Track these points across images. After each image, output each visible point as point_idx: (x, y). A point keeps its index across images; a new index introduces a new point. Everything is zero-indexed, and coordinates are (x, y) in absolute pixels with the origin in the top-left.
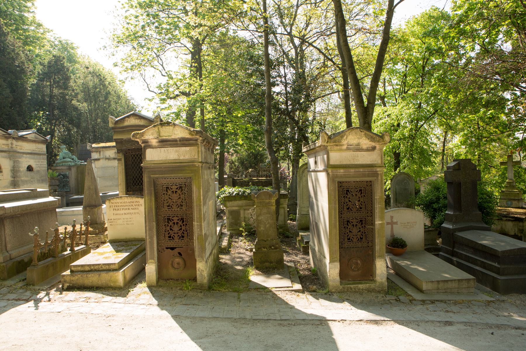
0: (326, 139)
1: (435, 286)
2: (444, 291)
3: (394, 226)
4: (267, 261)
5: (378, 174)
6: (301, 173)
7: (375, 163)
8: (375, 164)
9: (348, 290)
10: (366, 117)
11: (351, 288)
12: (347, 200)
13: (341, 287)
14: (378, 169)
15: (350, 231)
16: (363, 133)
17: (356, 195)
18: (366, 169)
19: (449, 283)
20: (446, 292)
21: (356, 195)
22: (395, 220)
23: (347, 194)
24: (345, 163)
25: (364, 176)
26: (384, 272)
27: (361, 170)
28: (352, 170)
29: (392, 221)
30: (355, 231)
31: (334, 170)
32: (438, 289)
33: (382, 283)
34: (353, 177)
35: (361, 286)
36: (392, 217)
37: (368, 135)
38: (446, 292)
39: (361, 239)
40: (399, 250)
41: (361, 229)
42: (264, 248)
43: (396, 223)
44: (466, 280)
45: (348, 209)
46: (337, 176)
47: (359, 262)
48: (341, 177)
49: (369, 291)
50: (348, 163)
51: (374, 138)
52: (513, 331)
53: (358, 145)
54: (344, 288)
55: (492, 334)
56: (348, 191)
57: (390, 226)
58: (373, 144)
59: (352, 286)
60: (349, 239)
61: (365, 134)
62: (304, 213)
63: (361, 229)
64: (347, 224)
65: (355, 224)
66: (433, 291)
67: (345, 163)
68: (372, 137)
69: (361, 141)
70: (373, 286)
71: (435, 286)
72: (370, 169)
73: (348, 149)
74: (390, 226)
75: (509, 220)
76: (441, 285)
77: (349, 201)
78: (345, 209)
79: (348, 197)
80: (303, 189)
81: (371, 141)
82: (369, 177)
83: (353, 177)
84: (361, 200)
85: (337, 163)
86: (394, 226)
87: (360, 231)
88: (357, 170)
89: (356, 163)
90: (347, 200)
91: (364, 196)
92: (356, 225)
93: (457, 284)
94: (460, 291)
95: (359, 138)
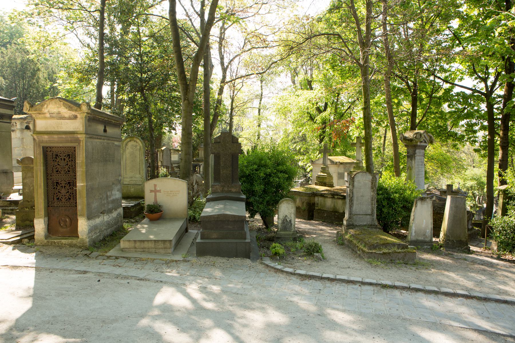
0: (28, 108)
1: (132, 245)
2: (142, 250)
3: (158, 194)
4: (27, 220)
5: (80, 140)
6: (124, 146)
7: (78, 130)
8: (77, 131)
9: (51, 244)
10: (186, 94)
11: (55, 243)
12: (56, 164)
13: (46, 241)
14: (79, 136)
15: (59, 192)
16: (62, 103)
17: (64, 159)
18: (69, 136)
19: (146, 243)
20: (143, 251)
21: (64, 159)
22: (158, 189)
23: (56, 158)
24: (50, 130)
25: (67, 142)
26: (84, 229)
27: (64, 136)
28: (56, 136)
29: (155, 189)
30: (63, 191)
31: (40, 136)
32: (135, 248)
33: (82, 240)
34: (57, 142)
35: (64, 241)
36: (155, 186)
37: (66, 104)
38: (144, 251)
39: (70, 199)
40: (155, 215)
41: (69, 190)
42: (26, 208)
43: (159, 191)
44: (162, 241)
45: (57, 171)
46: (42, 142)
47: (67, 220)
48: (46, 142)
49: (71, 246)
50: (53, 130)
51: (72, 108)
52: (76, 276)
53: (59, 113)
54: (48, 242)
55: (99, 281)
56: (56, 155)
57: (153, 194)
58: (74, 113)
59: (56, 241)
60: (58, 199)
61: (64, 104)
62: (127, 183)
63: (69, 190)
64: (57, 185)
65: (63, 185)
66: (131, 249)
67: (50, 130)
68: (70, 107)
69: (60, 110)
70: (74, 241)
71: (132, 245)
72: (71, 136)
73: (52, 117)
74: (153, 194)
75: (339, 198)
76: (138, 244)
77: (58, 164)
78: (55, 172)
79: (57, 161)
80: (126, 160)
81: (69, 110)
82: (71, 142)
83: (57, 142)
84: (69, 164)
85: (43, 130)
86: (158, 194)
87: (68, 192)
88: (60, 136)
89: (60, 130)
90: (56, 164)
91: (72, 160)
92: (65, 186)
93: (153, 244)
94: (157, 251)
95: (58, 108)
